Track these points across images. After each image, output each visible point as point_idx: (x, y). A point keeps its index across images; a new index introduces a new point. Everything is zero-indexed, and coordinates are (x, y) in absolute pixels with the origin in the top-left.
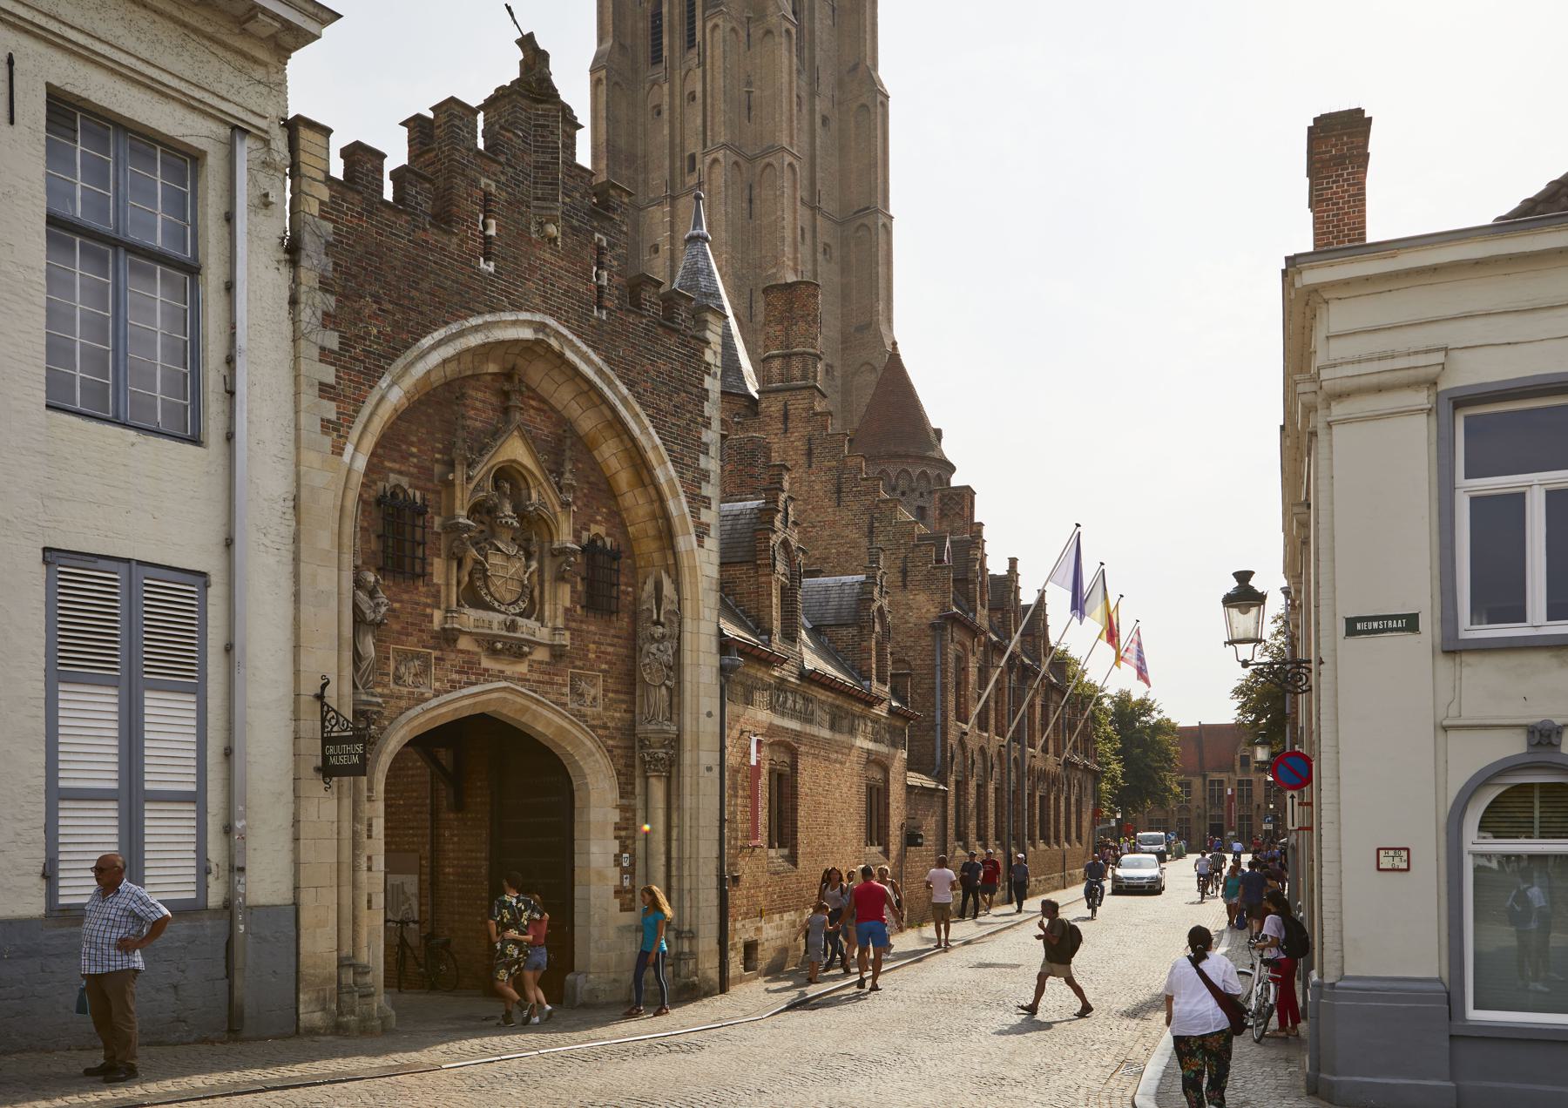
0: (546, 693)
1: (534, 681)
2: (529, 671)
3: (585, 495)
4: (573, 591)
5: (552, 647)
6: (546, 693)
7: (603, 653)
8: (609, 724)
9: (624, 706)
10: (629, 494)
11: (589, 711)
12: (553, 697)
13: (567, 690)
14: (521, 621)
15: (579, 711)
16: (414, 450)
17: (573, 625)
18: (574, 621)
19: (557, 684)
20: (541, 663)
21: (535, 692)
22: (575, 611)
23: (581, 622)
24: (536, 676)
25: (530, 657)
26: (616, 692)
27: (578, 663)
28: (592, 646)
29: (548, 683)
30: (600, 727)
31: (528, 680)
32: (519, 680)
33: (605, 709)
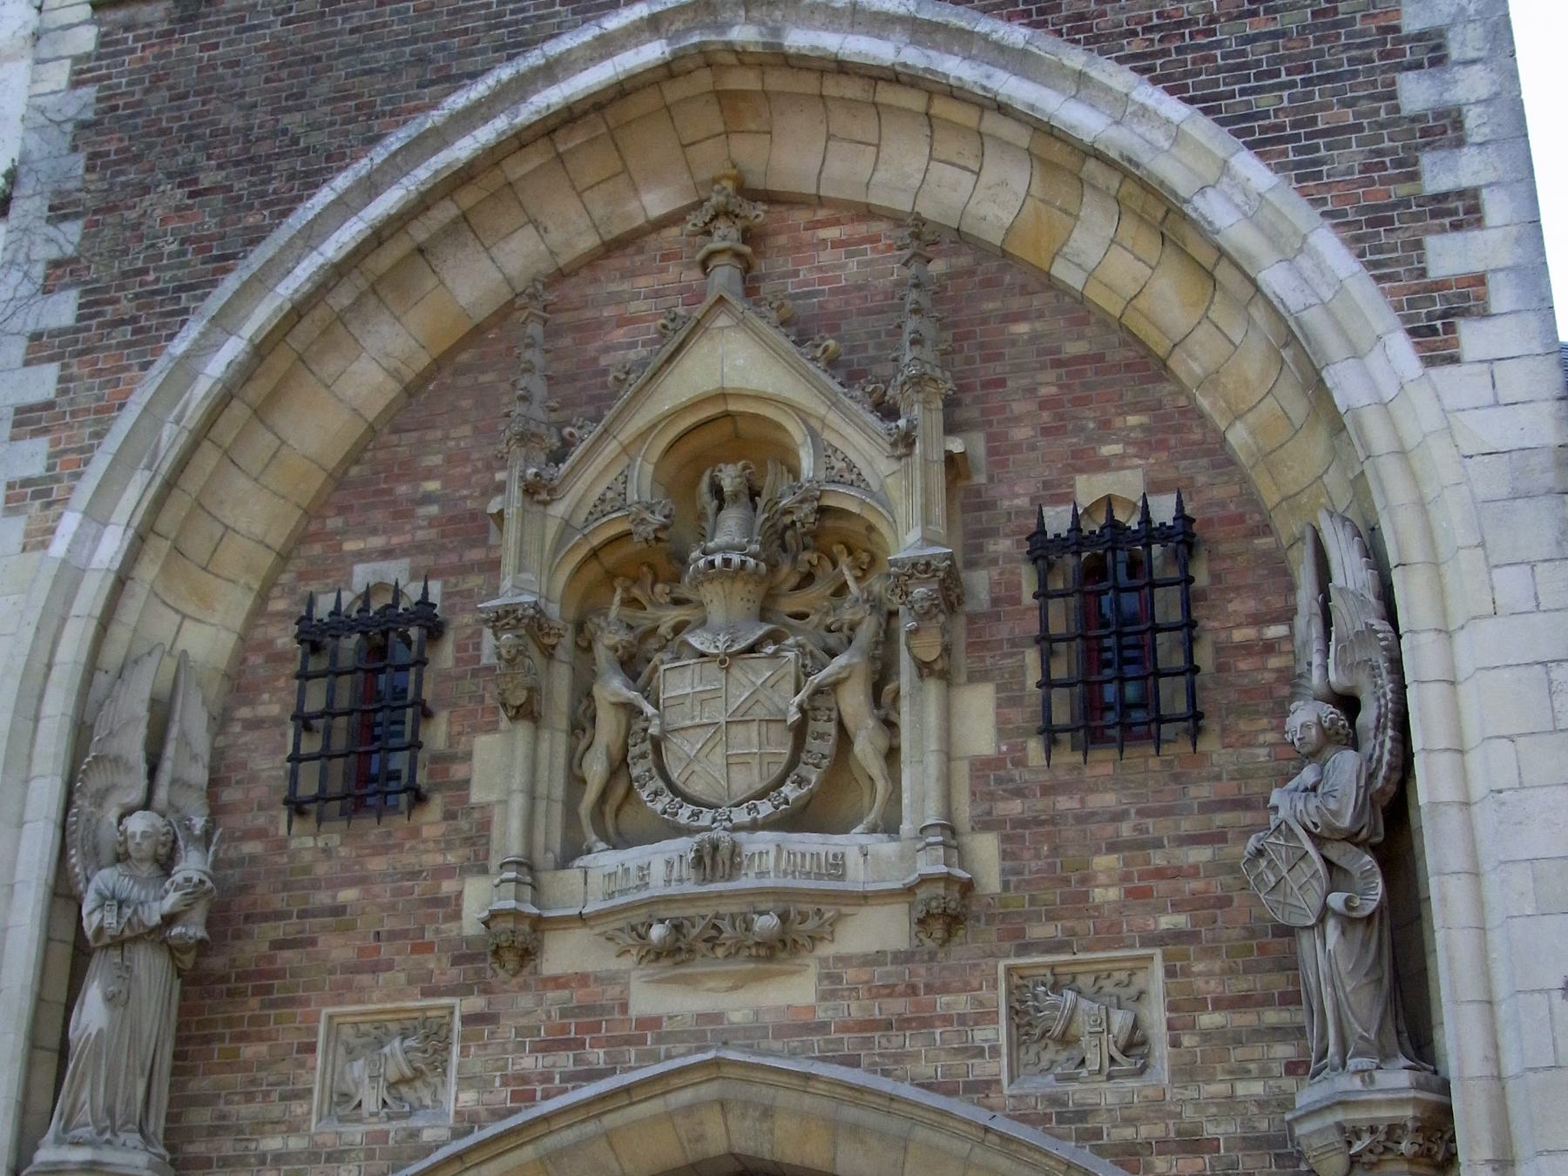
0: (899, 1058)
1: (844, 1028)
2: (823, 996)
3: (1044, 404)
4: (1008, 699)
5: (910, 890)
6: (899, 1058)
7: (1159, 873)
8: (1210, 1130)
9: (1284, 1051)
10: (1200, 334)
11: (1107, 1094)
12: (925, 1069)
13: (999, 1033)
14: (765, 841)
15: (1054, 1100)
16: (432, 486)
17: (1015, 807)
18: (1019, 793)
19: (947, 1020)
20: (874, 959)
21: (852, 1062)
22: (1020, 763)
23: (1048, 790)
24: (856, 1010)
25: (826, 950)
26: (1240, 1002)
27: (1039, 931)
28: (1104, 862)
29: (904, 1023)
30: (1163, 1146)
31: (822, 1027)
32: (781, 1031)
33: (1186, 1072)
